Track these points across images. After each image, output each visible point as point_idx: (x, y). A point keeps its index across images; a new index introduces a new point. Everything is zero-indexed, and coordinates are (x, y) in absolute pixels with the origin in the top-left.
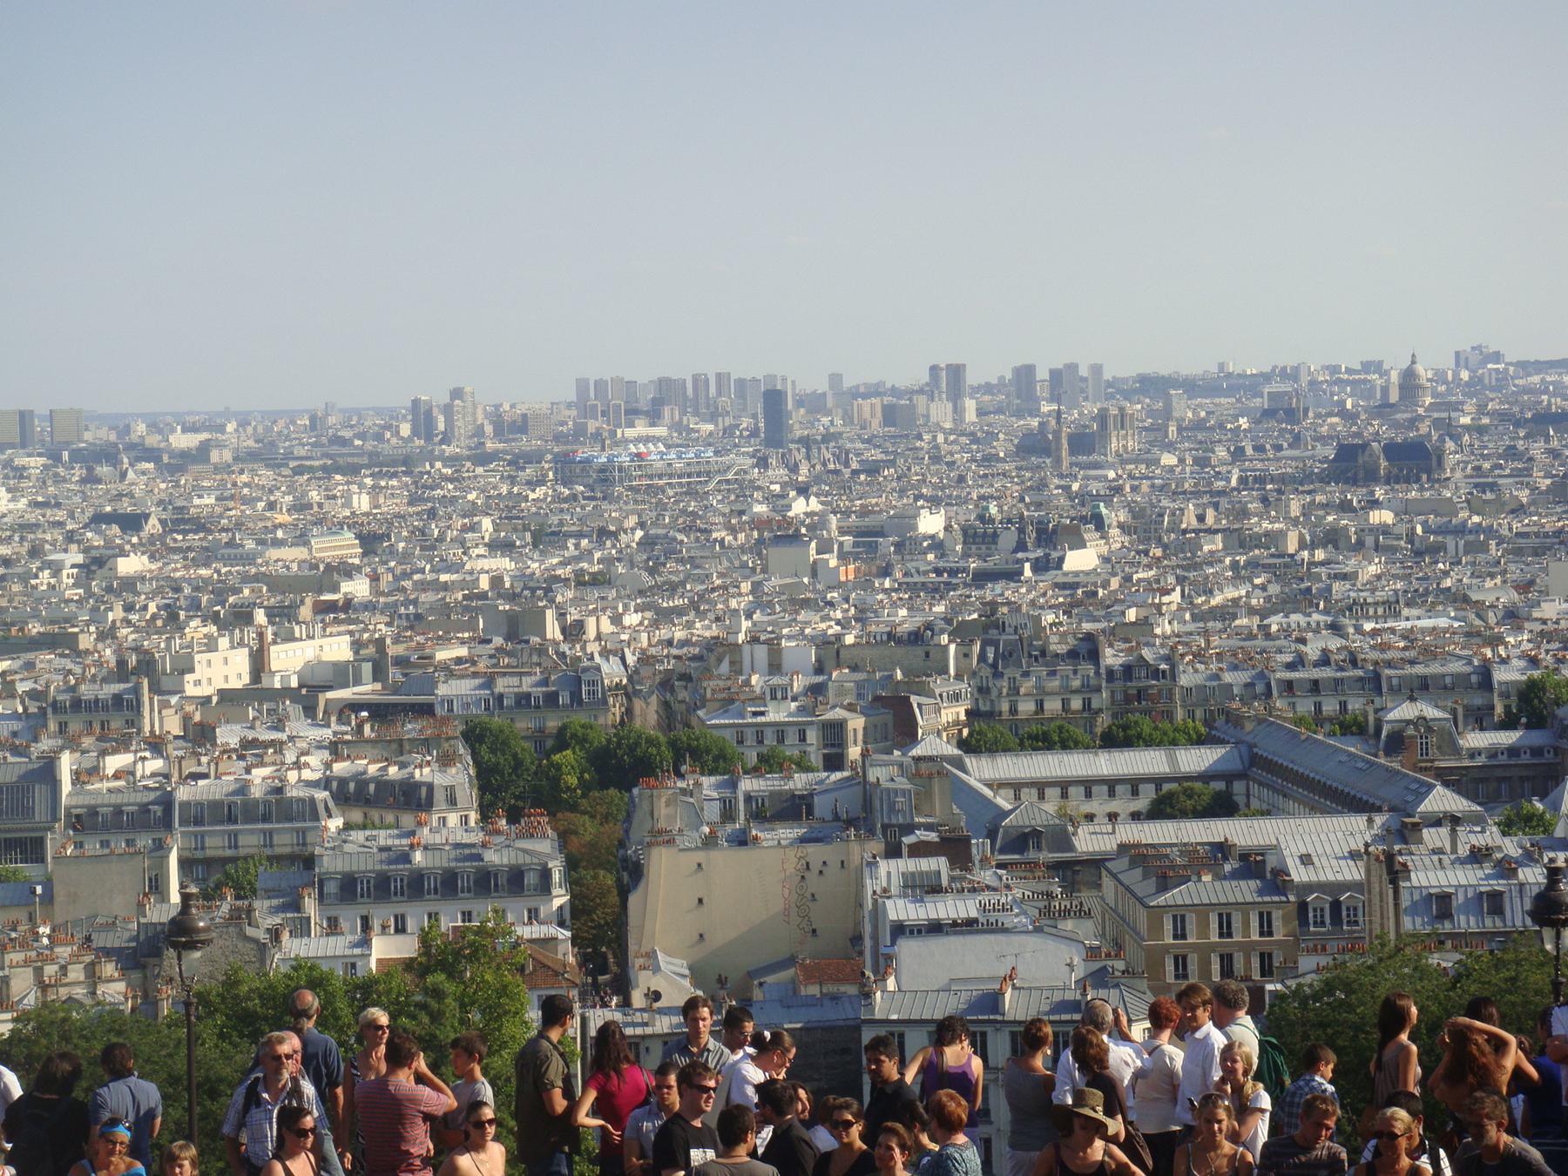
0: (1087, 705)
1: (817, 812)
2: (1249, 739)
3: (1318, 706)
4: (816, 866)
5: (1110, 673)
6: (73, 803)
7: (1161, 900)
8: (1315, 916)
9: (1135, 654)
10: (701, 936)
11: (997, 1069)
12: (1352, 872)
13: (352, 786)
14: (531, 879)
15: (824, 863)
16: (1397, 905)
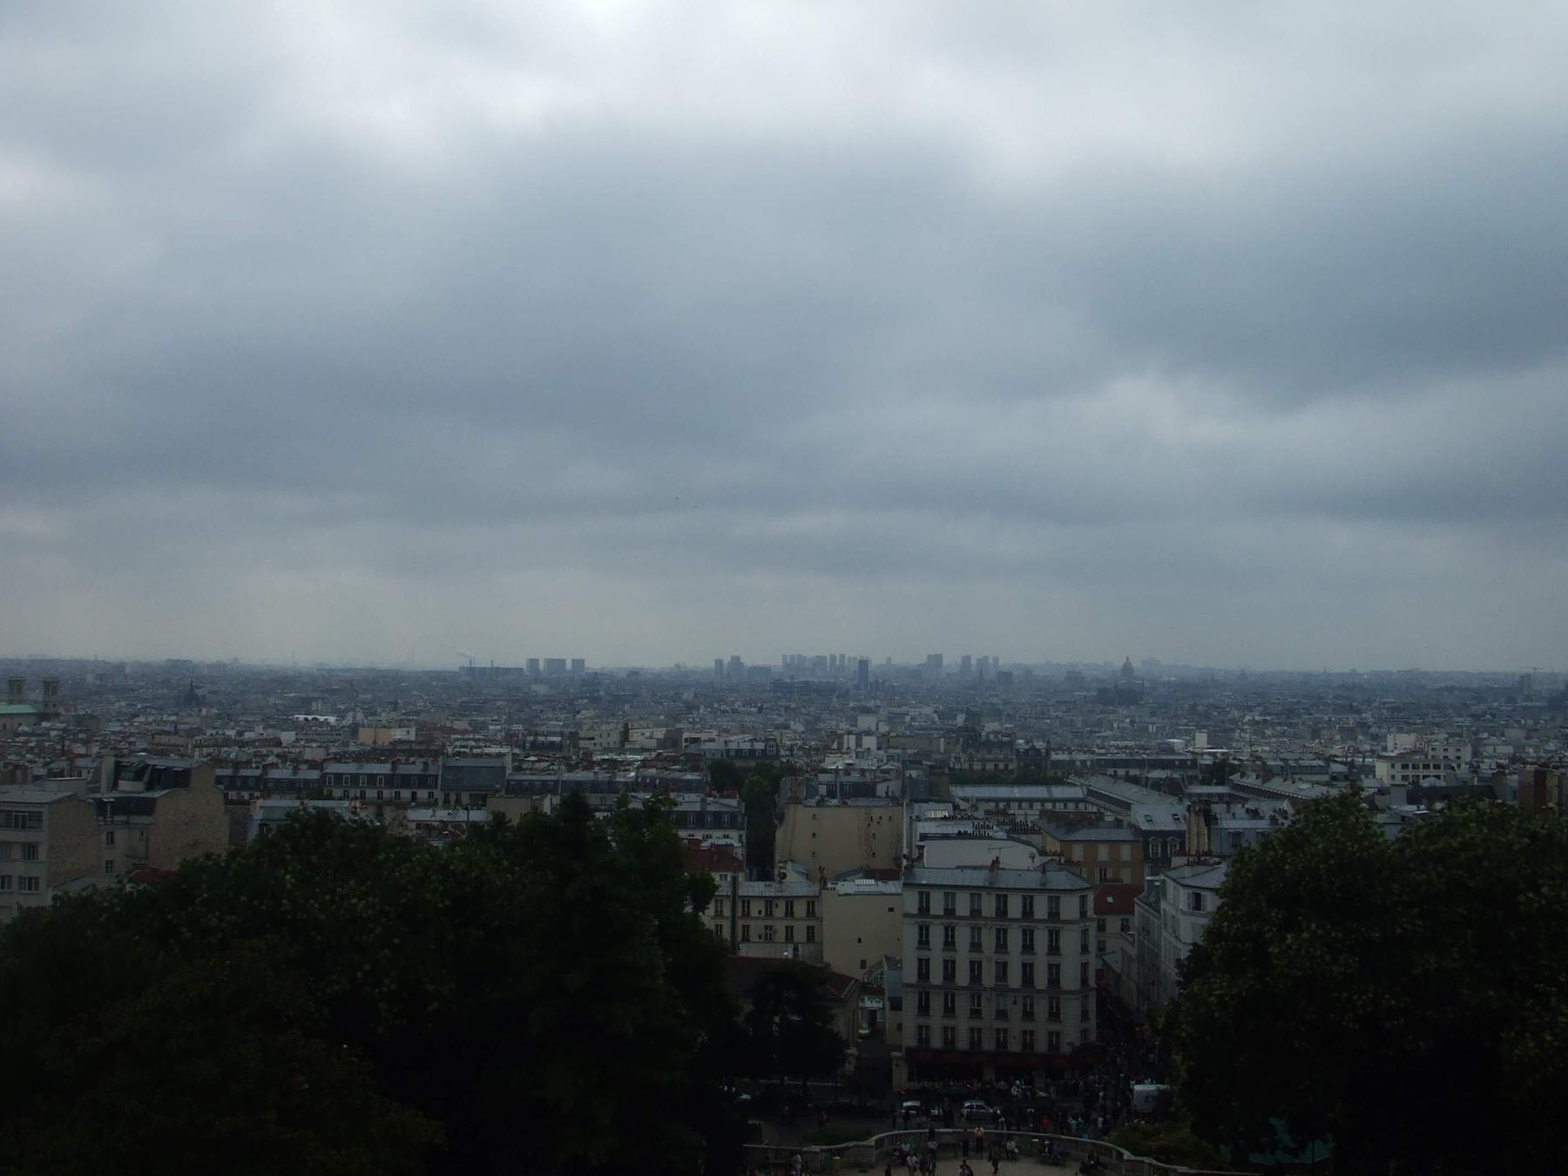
0: (1006, 766)
1: (879, 793)
2: (1086, 783)
3: (1115, 772)
4: (876, 819)
5: (1017, 750)
6: (512, 777)
7: (1068, 839)
8: (1153, 850)
9: (1031, 744)
10: (814, 853)
11: (987, 918)
12: (1172, 827)
13: (648, 780)
14: (726, 818)
15: (881, 818)
16: (1209, 839)
